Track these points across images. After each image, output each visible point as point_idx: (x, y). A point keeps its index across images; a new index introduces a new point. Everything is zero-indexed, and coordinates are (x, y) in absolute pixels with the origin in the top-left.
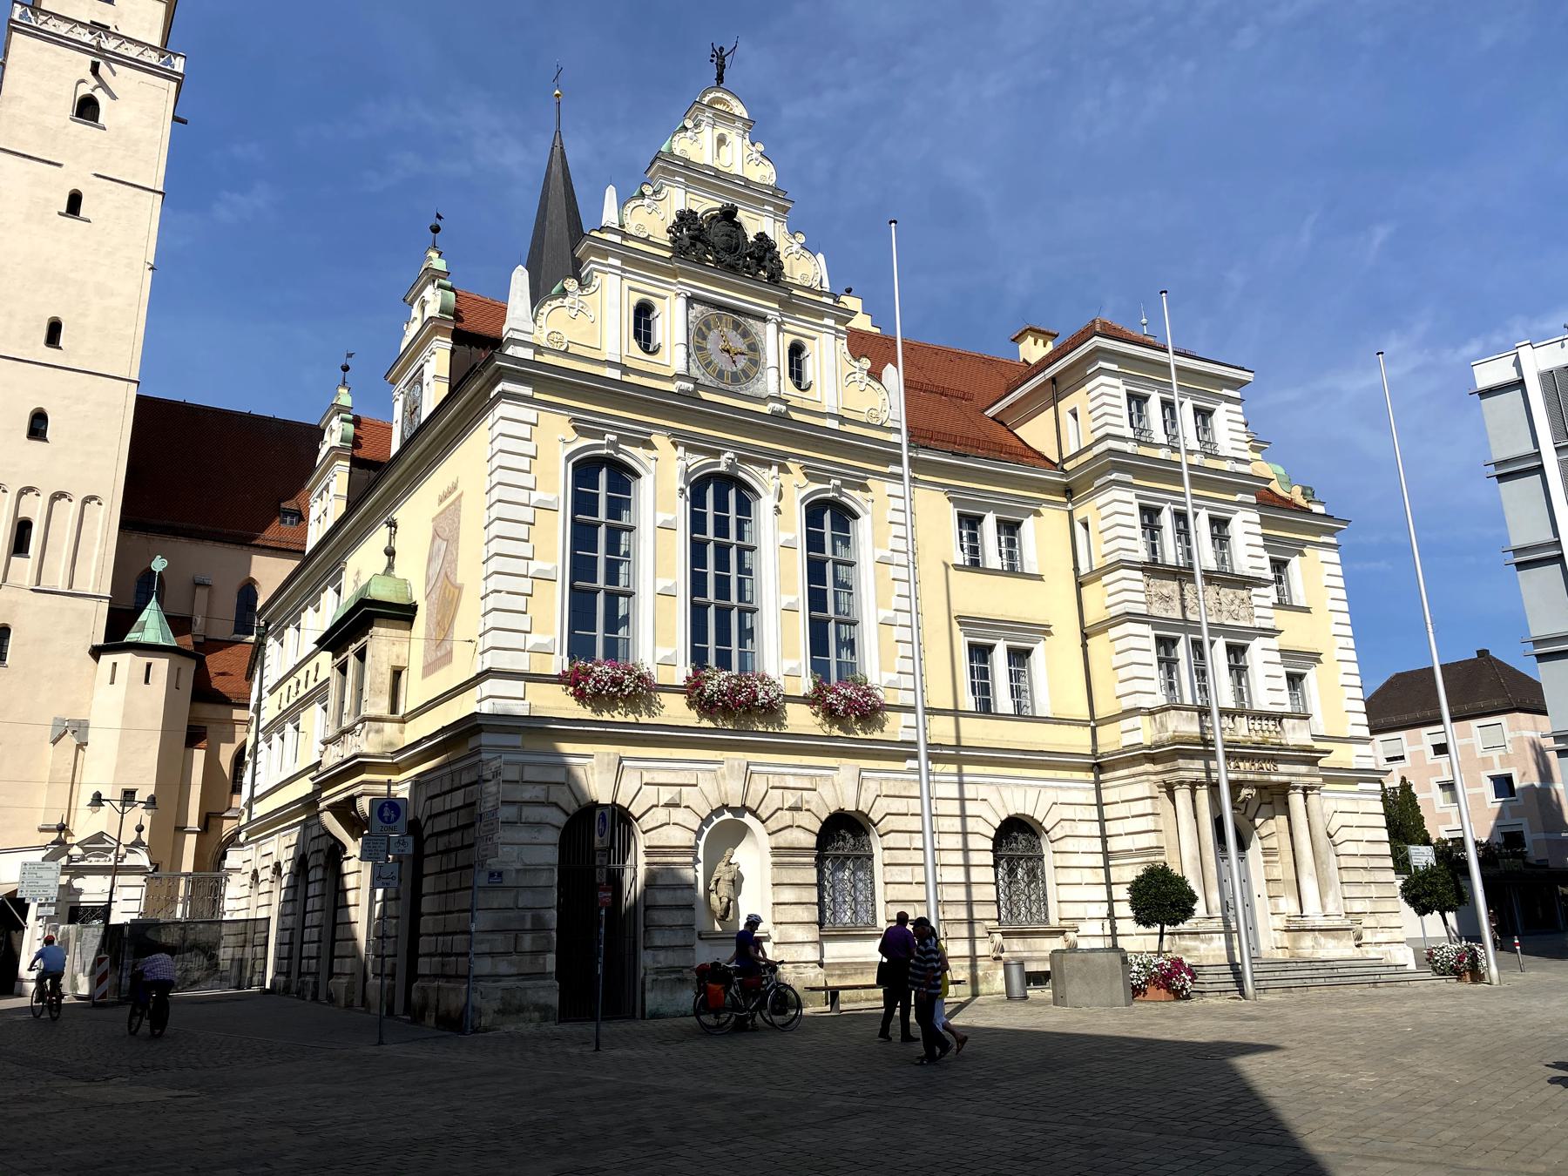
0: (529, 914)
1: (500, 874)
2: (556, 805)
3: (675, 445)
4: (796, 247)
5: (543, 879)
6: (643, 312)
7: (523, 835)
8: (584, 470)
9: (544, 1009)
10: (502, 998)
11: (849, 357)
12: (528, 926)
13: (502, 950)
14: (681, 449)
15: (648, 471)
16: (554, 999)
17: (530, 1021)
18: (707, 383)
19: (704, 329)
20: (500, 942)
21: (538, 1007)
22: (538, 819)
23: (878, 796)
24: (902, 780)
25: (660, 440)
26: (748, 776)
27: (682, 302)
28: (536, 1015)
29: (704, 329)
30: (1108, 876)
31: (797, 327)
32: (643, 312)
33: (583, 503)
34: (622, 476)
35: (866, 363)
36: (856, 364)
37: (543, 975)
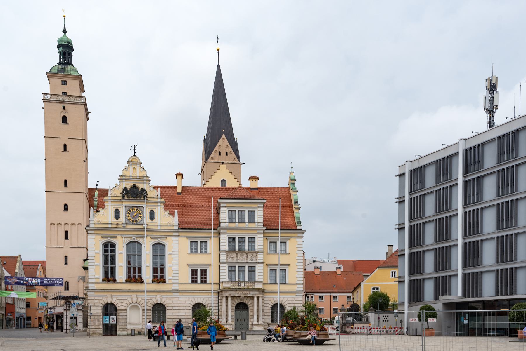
0: (97, 320)
1: (92, 314)
2: (101, 303)
3: (122, 237)
4: (152, 189)
5: (99, 314)
6: (117, 212)
7: (95, 308)
8: (106, 245)
9: (100, 334)
10: (93, 332)
11: (164, 211)
12: (97, 321)
13: (93, 325)
14: (124, 238)
15: (117, 244)
16: (102, 332)
17: (98, 335)
18: (130, 223)
19: (129, 212)
20: (92, 323)
21: (98, 333)
22: (98, 305)
23: (166, 300)
24: (171, 297)
25: (119, 237)
26: (137, 298)
27: (124, 208)
28: (98, 334)
29: (129, 212)
30: (218, 314)
31: (151, 207)
32: (117, 212)
33: (106, 251)
34: (113, 245)
35: (168, 212)
36: (165, 212)
37: (100, 328)
